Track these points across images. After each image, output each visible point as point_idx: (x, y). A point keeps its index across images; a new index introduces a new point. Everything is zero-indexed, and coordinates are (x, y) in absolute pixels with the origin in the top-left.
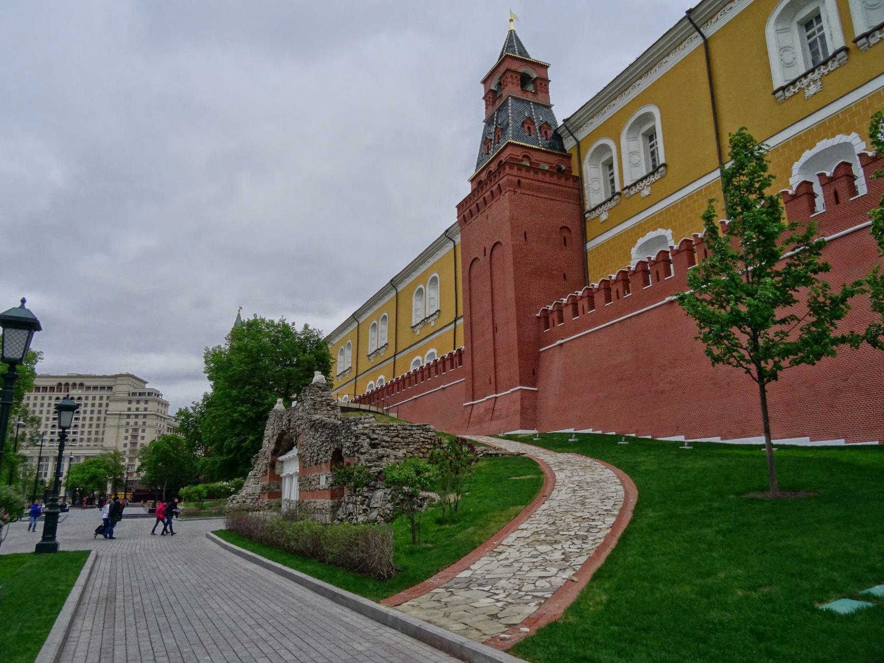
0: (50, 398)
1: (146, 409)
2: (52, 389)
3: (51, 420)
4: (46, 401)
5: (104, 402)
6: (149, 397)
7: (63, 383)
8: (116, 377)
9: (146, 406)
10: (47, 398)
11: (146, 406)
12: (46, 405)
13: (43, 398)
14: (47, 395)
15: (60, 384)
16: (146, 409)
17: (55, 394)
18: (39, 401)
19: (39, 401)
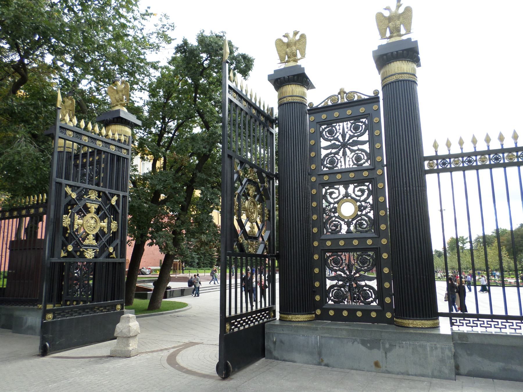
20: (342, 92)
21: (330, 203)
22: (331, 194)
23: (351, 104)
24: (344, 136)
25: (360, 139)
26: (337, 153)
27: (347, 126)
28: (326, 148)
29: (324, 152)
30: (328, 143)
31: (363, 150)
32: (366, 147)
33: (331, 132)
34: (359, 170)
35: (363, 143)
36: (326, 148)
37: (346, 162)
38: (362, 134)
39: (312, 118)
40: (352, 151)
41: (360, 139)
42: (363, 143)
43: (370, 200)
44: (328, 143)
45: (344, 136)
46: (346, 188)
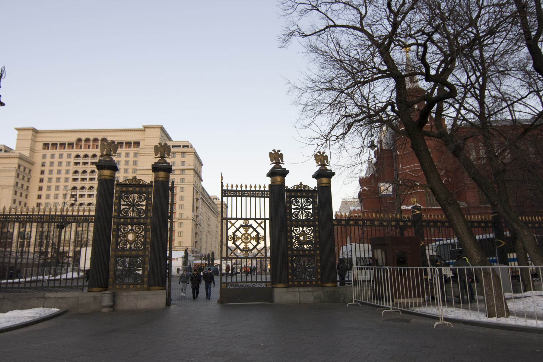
0: (69, 156)
1: (183, 163)
2: (71, 145)
3: (70, 180)
4: (65, 160)
5: (131, 159)
6: (185, 149)
7: (84, 138)
8: (145, 127)
9: (183, 159)
10: (65, 155)
11: (183, 159)
12: (64, 164)
13: (61, 156)
14: (65, 152)
15: (79, 140)
16: (183, 163)
17: (74, 152)
18: (56, 160)
19: (56, 160)
20: (301, 184)
21: (296, 234)
22: (296, 230)
23: (305, 191)
24: (302, 204)
25: (309, 207)
26: (299, 212)
27: (303, 200)
28: (294, 209)
29: (293, 211)
30: (295, 207)
31: (310, 212)
32: (311, 211)
33: (296, 202)
34: (308, 220)
35: (310, 209)
36: (294, 209)
37: (302, 217)
38: (310, 205)
39: (288, 194)
40: (305, 212)
41: (309, 207)
42: (310, 209)
43: (313, 234)
44: (295, 207)
45: (302, 204)
46: (303, 228)
